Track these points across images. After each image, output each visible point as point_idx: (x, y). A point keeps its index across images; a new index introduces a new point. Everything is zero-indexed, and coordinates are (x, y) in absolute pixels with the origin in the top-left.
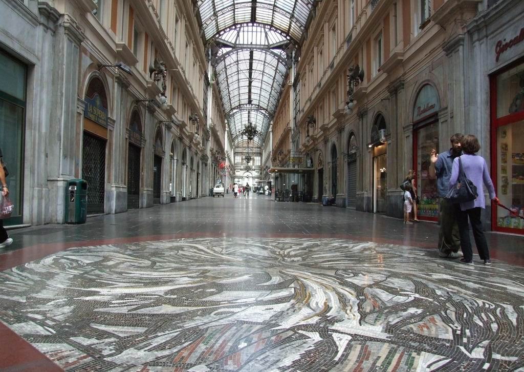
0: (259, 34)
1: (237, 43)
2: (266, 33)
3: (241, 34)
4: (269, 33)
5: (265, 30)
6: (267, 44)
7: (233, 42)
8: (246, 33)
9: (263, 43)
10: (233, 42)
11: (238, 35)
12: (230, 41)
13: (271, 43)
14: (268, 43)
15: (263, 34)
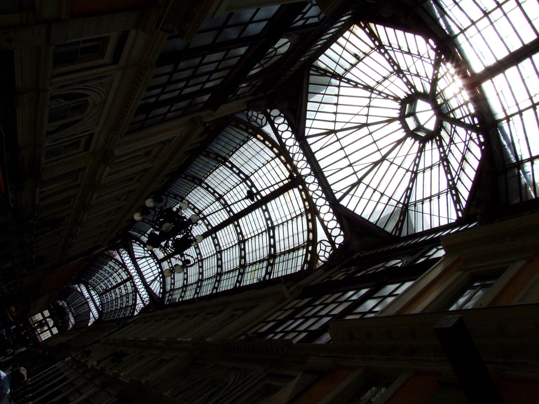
0: (151, 274)
1: (137, 260)
2: (156, 279)
3: (144, 260)
4: (156, 282)
5: (158, 276)
6: (148, 283)
7: (136, 257)
8: (146, 263)
9: (147, 280)
10: (136, 257)
11: (142, 258)
12: (135, 253)
13: (151, 287)
14: (150, 284)
15: (153, 278)
